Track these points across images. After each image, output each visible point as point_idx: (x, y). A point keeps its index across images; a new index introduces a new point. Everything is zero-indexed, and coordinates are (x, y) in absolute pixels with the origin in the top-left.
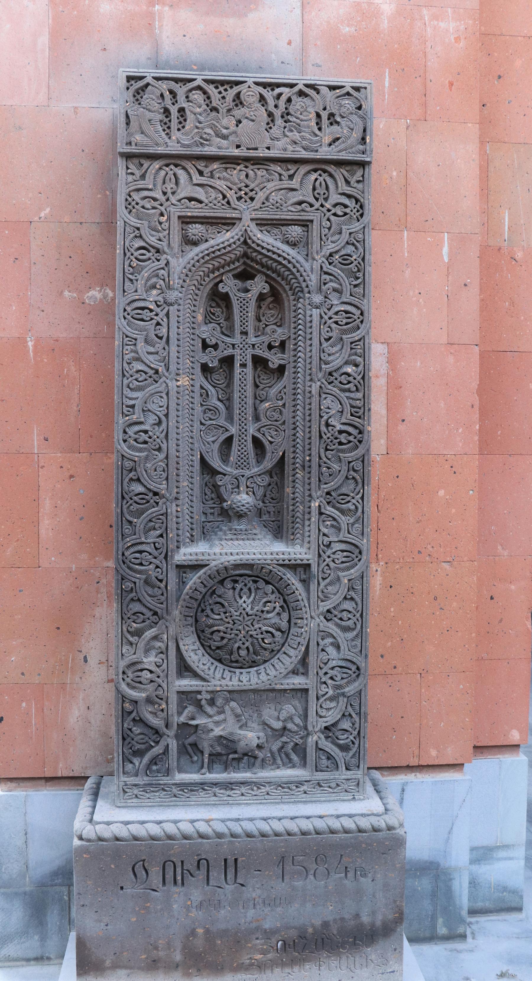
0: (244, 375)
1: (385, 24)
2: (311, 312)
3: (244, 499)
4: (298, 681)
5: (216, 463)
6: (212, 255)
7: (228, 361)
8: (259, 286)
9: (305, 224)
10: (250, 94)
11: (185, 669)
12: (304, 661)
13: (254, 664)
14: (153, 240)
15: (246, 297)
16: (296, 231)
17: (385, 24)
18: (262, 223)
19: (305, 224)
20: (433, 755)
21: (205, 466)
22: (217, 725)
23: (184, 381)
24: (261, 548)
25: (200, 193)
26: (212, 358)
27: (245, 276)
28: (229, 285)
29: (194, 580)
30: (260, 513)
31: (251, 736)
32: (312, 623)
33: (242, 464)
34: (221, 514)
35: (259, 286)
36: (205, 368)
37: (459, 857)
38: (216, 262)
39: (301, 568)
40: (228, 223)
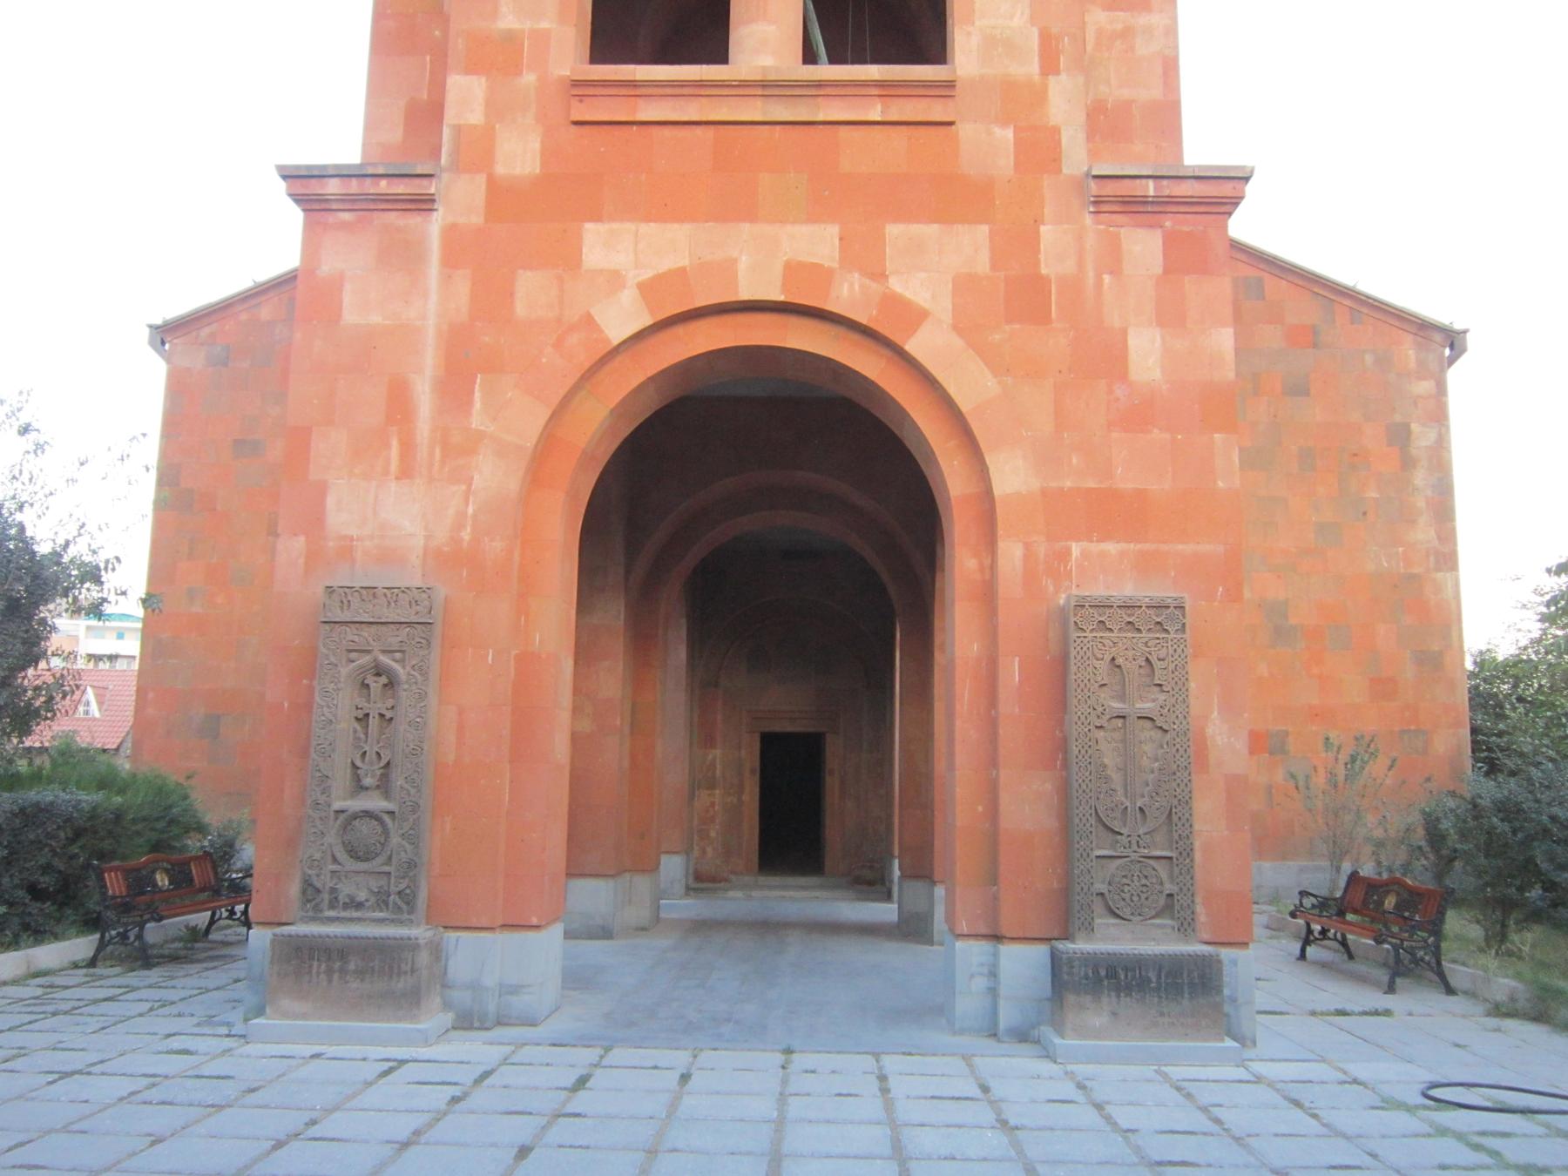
0: (374, 722)
1: (465, 544)
2: (405, 695)
3: (368, 781)
4: (386, 869)
5: (358, 763)
6: (362, 667)
7: (367, 715)
8: (384, 680)
9: (402, 652)
10: (380, 592)
11: (335, 860)
12: (390, 858)
13: (367, 860)
14: (333, 659)
15: (377, 685)
16: (398, 655)
17: (465, 544)
18: (384, 652)
19: (402, 652)
20: (474, 922)
21: (353, 764)
22: (345, 889)
23: (343, 725)
24: (375, 803)
25: (356, 639)
26: (360, 714)
27: (378, 674)
28: (370, 680)
29: (342, 817)
30: (378, 787)
31: (362, 896)
32: (395, 840)
33: (371, 763)
34: (359, 788)
35: (384, 680)
36: (357, 719)
37: (490, 981)
38: (363, 670)
39: (391, 813)
40: (369, 652)
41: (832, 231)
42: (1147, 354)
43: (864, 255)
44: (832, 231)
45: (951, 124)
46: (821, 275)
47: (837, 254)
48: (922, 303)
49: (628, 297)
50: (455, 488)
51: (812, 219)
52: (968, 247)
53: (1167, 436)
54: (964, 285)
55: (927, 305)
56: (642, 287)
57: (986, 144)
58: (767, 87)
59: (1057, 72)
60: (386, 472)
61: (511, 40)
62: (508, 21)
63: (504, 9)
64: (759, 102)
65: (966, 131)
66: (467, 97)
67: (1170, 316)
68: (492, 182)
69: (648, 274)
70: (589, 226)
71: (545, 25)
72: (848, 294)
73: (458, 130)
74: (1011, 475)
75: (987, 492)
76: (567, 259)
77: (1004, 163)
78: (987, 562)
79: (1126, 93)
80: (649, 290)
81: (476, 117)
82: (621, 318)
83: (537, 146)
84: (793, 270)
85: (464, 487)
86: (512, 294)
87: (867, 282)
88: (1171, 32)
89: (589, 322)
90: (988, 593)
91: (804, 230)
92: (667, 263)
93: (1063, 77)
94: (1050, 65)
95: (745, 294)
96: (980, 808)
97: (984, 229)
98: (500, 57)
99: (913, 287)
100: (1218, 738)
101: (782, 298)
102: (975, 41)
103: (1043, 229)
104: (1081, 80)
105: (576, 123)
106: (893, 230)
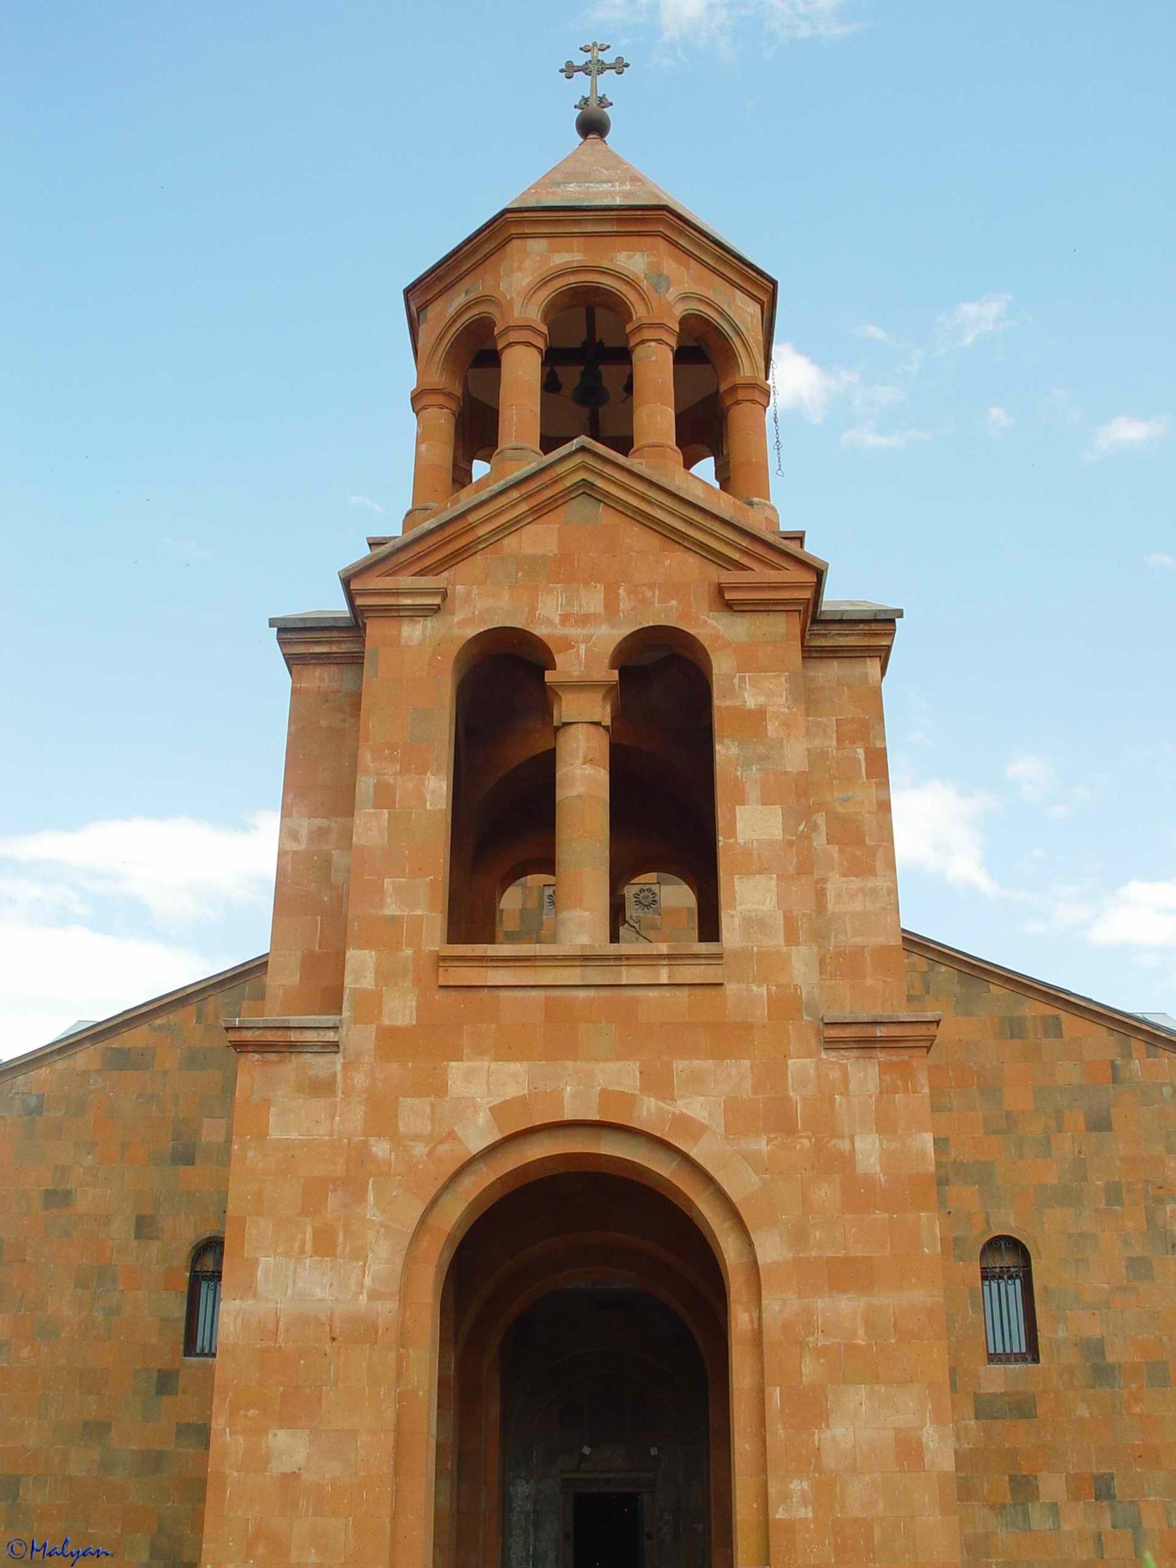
41: (634, 1066)
42: (868, 1151)
43: (658, 1082)
44: (634, 1066)
45: (721, 984)
46: (629, 1100)
47: (638, 1084)
48: (702, 1120)
49: (483, 1118)
50: (355, 1264)
51: (618, 1058)
52: (736, 1076)
53: (886, 1215)
54: (733, 1108)
55: (705, 1122)
56: (492, 1109)
57: (747, 995)
58: (585, 959)
59: (798, 944)
60: (302, 1252)
61: (393, 920)
62: (391, 909)
63: (389, 900)
64: (578, 971)
65: (731, 988)
66: (361, 967)
67: (885, 1125)
68: (379, 1027)
69: (497, 1101)
70: (452, 1064)
71: (418, 912)
72: (648, 1112)
73: (355, 991)
74: (771, 1249)
75: (754, 1266)
76: (440, 1089)
77: (761, 1013)
78: (755, 1315)
79: (859, 941)
80: (497, 1112)
81: (368, 983)
82: (478, 1134)
83: (414, 1003)
84: (606, 1096)
85: (361, 1263)
86: (396, 1116)
87: (662, 1104)
88: (893, 891)
89: (452, 1135)
90: (757, 1338)
91: (613, 1066)
92: (512, 1091)
93: (803, 949)
94: (791, 938)
95: (569, 1116)
96: (755, 1505)
97: (746, 1063)
98: (386, 934)
99: (695, 1107)
100: (931, 1444)
101: (598, 1118)
102: (737, 921)
103: (790, 1062)
104: (815, 948)
105: (441, 987)
106: (679, 1065)
